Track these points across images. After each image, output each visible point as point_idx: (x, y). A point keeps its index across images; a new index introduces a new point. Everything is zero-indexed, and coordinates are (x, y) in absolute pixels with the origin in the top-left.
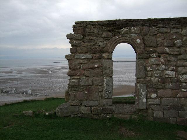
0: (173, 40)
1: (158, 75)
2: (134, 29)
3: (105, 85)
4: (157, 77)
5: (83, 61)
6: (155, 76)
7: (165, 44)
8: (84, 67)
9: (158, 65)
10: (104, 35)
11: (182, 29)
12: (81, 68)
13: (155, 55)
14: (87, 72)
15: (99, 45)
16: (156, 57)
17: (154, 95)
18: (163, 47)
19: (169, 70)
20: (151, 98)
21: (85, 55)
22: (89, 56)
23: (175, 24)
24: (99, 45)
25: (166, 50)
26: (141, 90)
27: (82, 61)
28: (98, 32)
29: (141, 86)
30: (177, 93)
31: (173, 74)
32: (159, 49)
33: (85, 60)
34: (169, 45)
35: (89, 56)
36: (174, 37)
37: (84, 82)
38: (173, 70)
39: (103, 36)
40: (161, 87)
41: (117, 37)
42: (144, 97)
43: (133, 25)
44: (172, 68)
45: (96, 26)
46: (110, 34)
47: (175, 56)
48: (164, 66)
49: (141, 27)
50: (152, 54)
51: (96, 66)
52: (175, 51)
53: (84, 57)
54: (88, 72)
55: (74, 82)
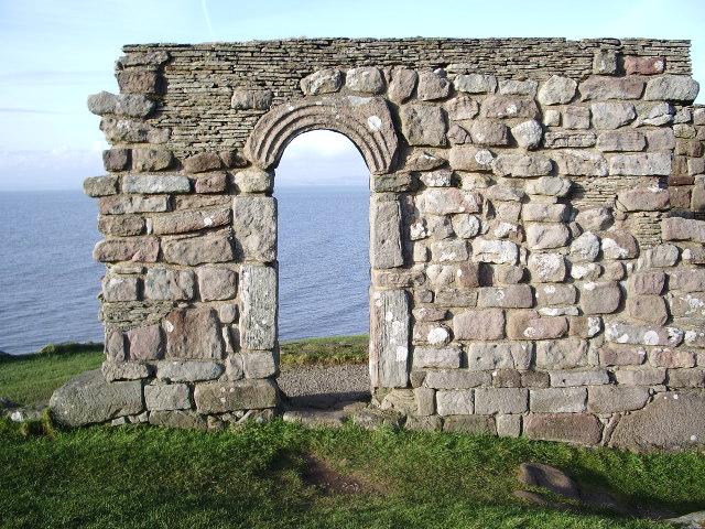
0: (509, 123)
1: (451, 256)
4: (447, 262)
5: (154, 200)
7: (479, 138)
8: (158, 229)
10: (240, 96)
11: (539, 81)
12: (149, 231)
17: (437, 334)
20: (425, 344)
21: (161, 177)
22: (177, 182)
24: (219, 136)
26: (389, 316)
28: (216, 86)
30: (525, 323)
35: (177, 182)
36: (512, 109)
37: (161, 287)
39: (234, 102)
41: (291, 109)
43: (353, 61)
44: (506, 227)
45: (208, 62)
51: (208, 222)
53: (160, 188)
54: (177, 245)
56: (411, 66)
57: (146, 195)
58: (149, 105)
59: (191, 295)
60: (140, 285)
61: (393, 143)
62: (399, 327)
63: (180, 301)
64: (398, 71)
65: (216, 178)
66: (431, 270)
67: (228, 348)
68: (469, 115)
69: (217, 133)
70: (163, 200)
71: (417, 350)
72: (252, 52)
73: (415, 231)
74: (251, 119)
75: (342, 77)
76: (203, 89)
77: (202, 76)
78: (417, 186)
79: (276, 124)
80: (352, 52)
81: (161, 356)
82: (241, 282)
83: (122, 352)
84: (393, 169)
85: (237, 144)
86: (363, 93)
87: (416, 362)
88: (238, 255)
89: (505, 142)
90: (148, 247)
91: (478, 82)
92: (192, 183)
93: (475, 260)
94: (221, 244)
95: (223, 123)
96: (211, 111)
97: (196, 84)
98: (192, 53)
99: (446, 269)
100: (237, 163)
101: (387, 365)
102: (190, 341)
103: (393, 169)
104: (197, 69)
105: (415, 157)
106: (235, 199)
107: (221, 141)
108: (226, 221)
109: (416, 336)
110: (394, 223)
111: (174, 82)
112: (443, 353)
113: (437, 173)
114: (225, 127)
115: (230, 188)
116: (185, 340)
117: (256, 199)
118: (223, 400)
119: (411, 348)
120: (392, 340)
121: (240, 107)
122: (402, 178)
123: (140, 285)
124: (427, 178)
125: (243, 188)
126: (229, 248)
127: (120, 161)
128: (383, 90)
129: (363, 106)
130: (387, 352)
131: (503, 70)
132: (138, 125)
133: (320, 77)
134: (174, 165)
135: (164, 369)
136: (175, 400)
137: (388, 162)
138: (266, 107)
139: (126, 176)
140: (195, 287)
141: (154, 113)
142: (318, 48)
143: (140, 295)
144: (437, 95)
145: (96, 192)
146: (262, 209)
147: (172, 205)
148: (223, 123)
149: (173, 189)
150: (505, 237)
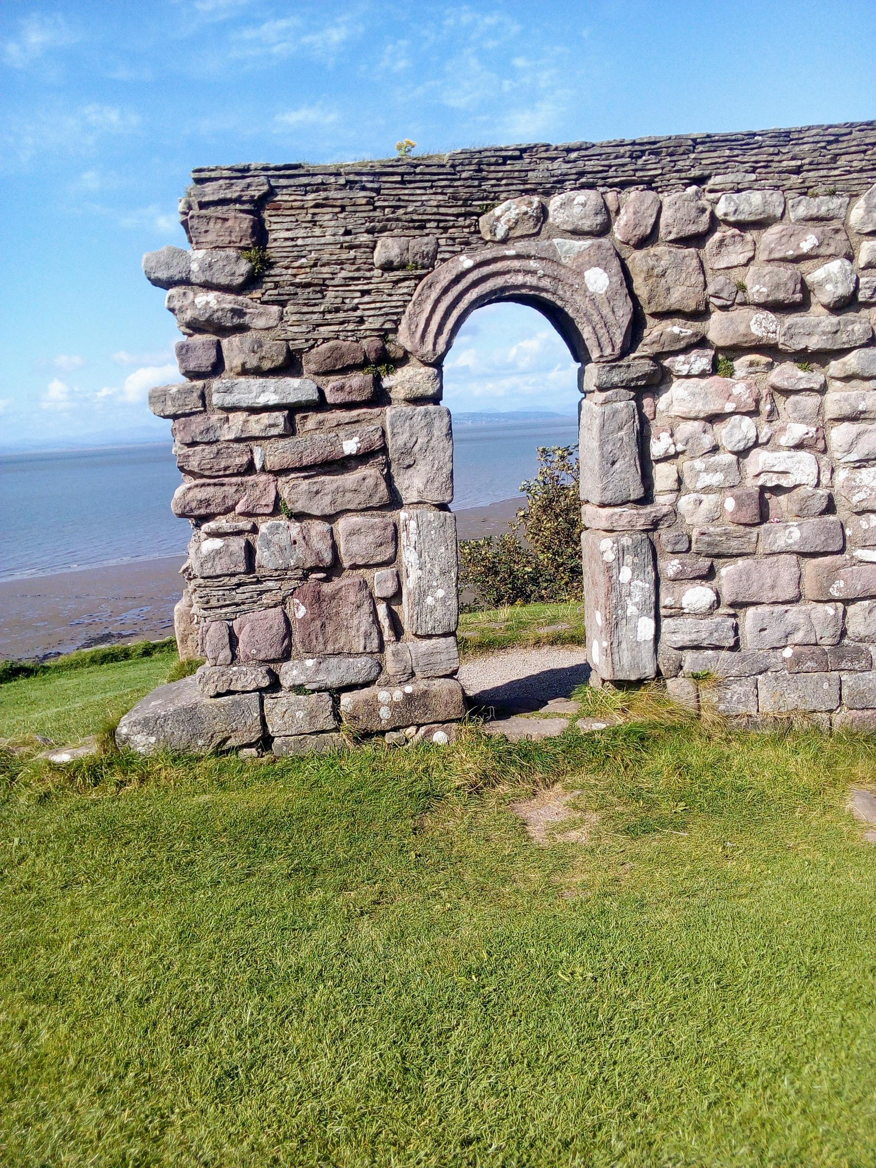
0: (804, 266)
1: (716, 479)
2: (573, 207)
3: (408, 556)
6: (699, 485)
8: (274, 462)
9: (714, 418)
10: (388, 247)
13: (700, 361)
14: (297, 491)
15: (359, 313)
16: (703, 375)
17: (698, 596)
18: (744, 311)
19: (778, 448)
20: (678, 612)
21: (272, 382)
22: (298, 388)
23: (815, 166)
24: (359, 313)
25: (762, 325)
26: (626, 574)
27: (257, 425)
28: (347, 233)
29: (622, 552)
30: (832, 574)
31: (802, 469)
32: (718, 329)
33: (279, 417)
34: (781, 296)
35: (298, 388)
36: (808, 244)
37: (282, 550)
38: (799, 446)
39: (379, 257)
40: (734, 546)
41: (468, 263)
42: (642, 612)
43: (558, 184)
44: (798, 431)
45: (332, 194)
46: (422, 244)
47: (823, 357)
48: (744, 429)
49: (611, 197)
50: (681, 358)
51: (350, 447)
52: (815, 327)
53: (272, 399)
54: (304, 485)
55: (218, 552)
56: (649, 184)
57: (254, 410)
58: (244, 267)
59: (328, 557)
60: (250, 551)
61: (624, 313)
62: (642, 587)
63: (315, 569)
64: (632, 195)
65: (358, 380)
66: (685, 503)
67: (387, 634)
68: (742, 259)
69: (355, 309)
70: (279, 417)
71: (665, 623)
72: (402, 174)
73: (657, 448)
74: (407, 283)
75: (544, 211)
76: (329, 239)
77: (325, 216)
78: (657, 381)
79: (445, 291)
80: (559, 167)
81: (286, 656)
82: (403, 535)
83: (227, 652)
84: (625, 352)
85: (388, 326)
86: (576, 233)
87: (665, 637)
88: (394, 502)
89: (798, 297)
90: (262, 490)
91: (752, 203)
92: (321, 392)
93: (752, 485)
94: (370, 482)
95: (364, 293)
96: (344, 274)
97: (317, 231)
98: (304, 180)
99: (709, 500)
100: (386, 360)
101: (624, 646)
102: (329, 629)
103: (625, 352)
104: (317, 206)
105: (655, 331)
106: (389, 411)
107: (361, 321)
108: (378, 444)
109: (666, 600)
110: (627, 435)
111: (279, 231)
112: (707, 623)
113: (694, 353)
114: (366, 299)
115: (379, 397)
116: (323, 625)
117: (421, 409)
118: (385, 713)
119: (657, 619)
120: (632, 610)
121: (388, 267)
122: (639, 365)
123: (250, 551)
124: (678, 364)
125: (399, 394)
126: (383, 486)
127: (206, 360)
128: (605, 230)
129: (580, 254)
130: (624, 630)
131: (795, 179)
132: (229, 301)
133: (508, 211)
134: (290, 365)
135: (290, 674)
136: (312, 716)
137: (619, 345)
138: (430, 261)
139: (216, 383)
140: (334, 547)
141: (252, 281)
142: (504, 164)
143: (251, 567)
144: (692, 229)
145: (170, 410)
146: (429, 425)
147: (290, 430)
148: (364, 293)
149: (291, 399)
150: (799, 446)
